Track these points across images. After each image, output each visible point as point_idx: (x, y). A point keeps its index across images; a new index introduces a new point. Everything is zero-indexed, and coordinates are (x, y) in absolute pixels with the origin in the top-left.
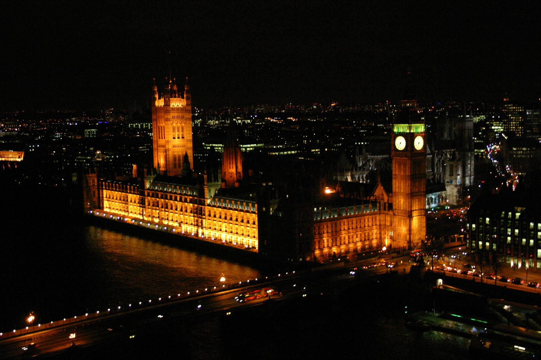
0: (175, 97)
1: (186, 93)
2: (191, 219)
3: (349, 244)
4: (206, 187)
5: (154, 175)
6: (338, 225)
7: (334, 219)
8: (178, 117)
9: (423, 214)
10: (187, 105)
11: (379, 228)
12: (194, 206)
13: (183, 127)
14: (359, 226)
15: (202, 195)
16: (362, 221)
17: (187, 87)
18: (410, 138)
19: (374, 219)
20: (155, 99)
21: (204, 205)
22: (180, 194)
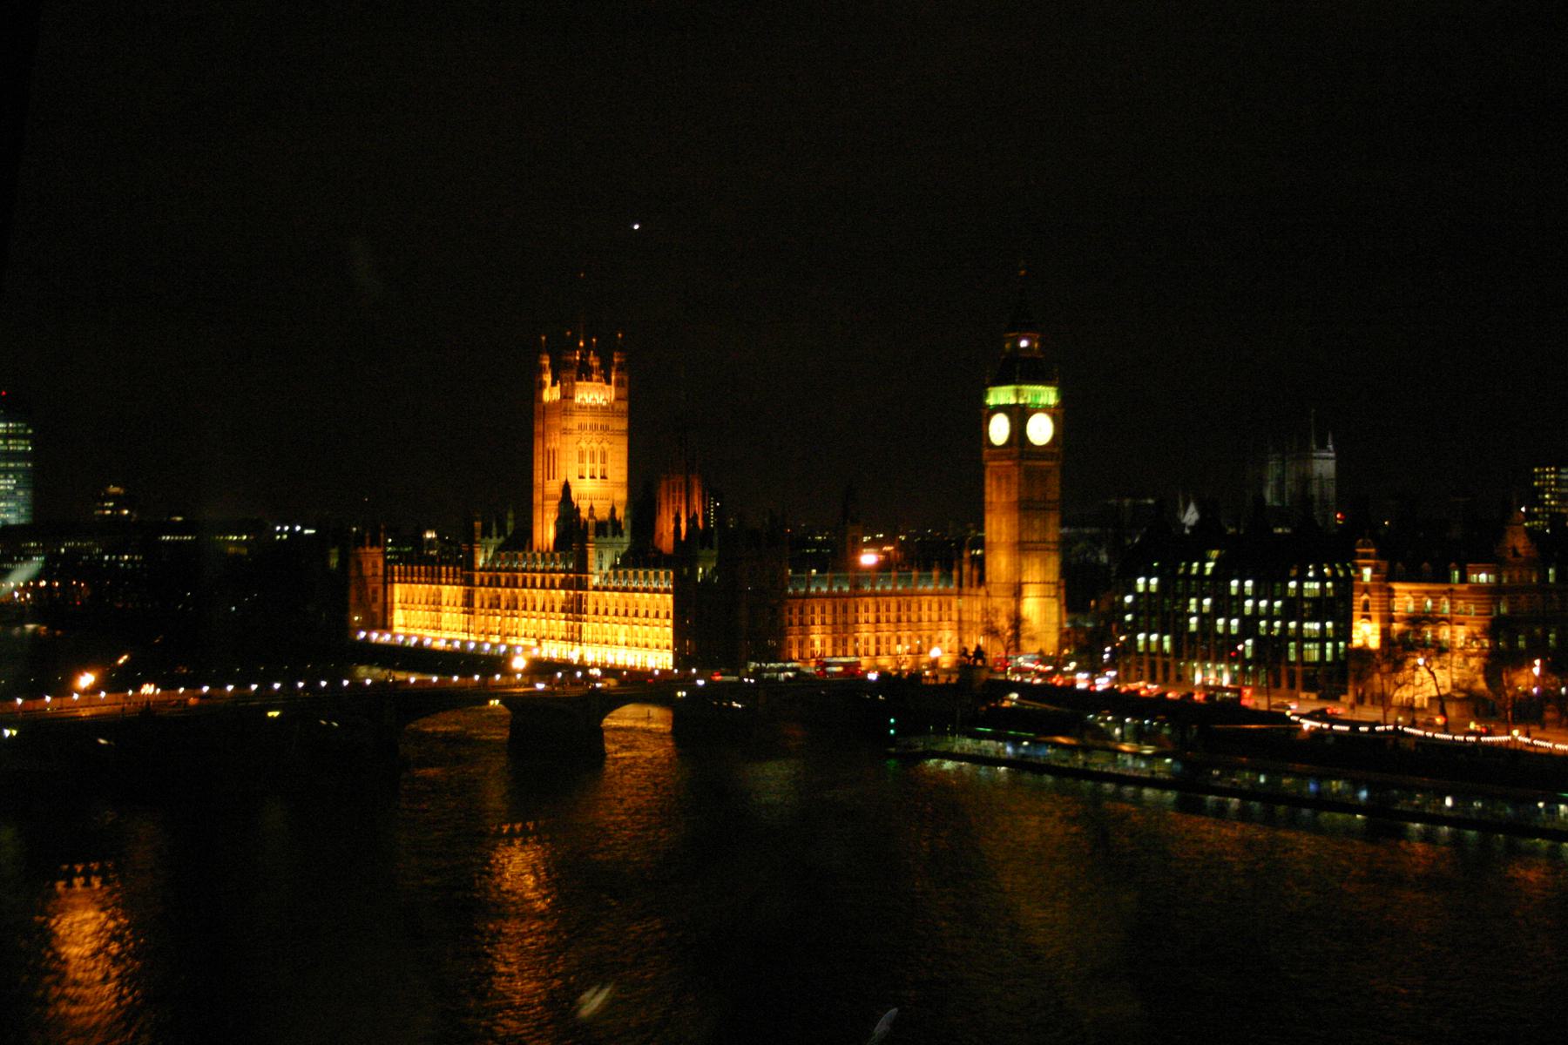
0: (590, 380)
1: (617, 371)
2: (559, 625)
3: (879, 657)
4: (592, 547)
5: (498, 536)
6: (851, 608)
7: (841, 595)
8: (594, 428)
9: (1052, 594)
10: (618, 399)
11: (956, 627)
12: (567, 595)
13: (604, 452)
14: (904, 618)
15: (582, 567)
16: (914, 607)
17: (618, 357)
18: (1019, 415)
19: (945, 607)
20: (542, 386)
21: (586, 589)
22: (543, 571)
